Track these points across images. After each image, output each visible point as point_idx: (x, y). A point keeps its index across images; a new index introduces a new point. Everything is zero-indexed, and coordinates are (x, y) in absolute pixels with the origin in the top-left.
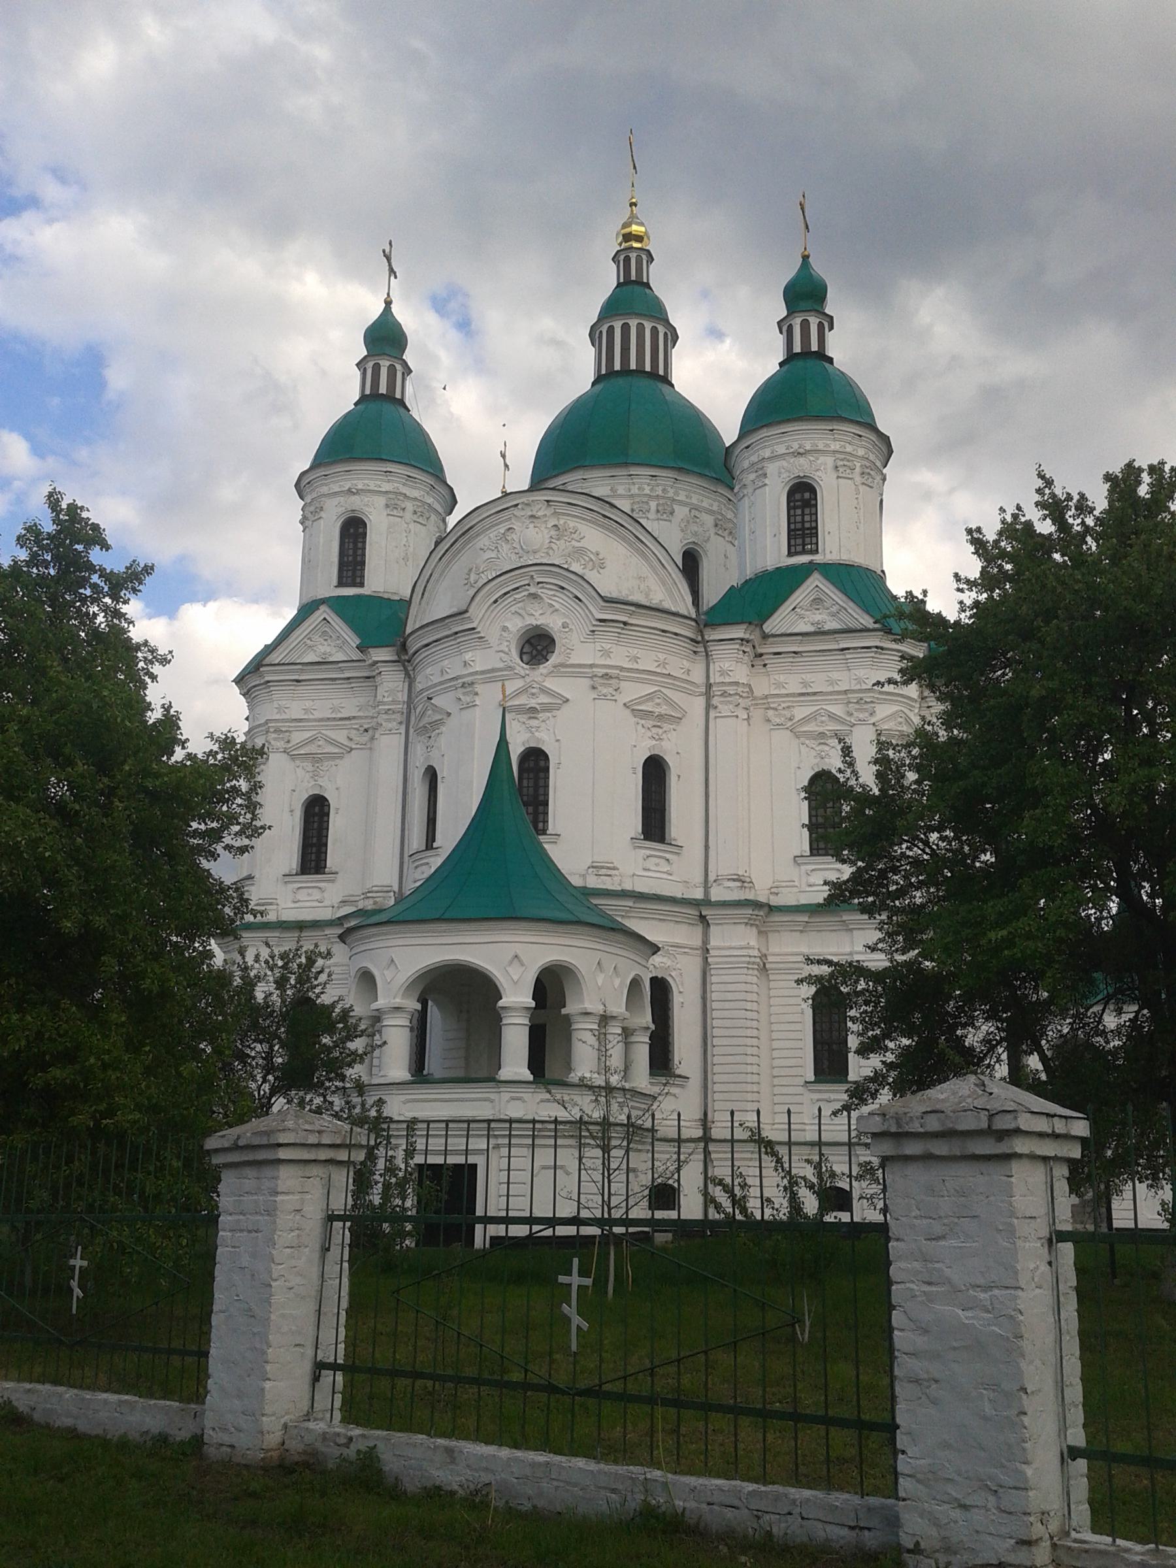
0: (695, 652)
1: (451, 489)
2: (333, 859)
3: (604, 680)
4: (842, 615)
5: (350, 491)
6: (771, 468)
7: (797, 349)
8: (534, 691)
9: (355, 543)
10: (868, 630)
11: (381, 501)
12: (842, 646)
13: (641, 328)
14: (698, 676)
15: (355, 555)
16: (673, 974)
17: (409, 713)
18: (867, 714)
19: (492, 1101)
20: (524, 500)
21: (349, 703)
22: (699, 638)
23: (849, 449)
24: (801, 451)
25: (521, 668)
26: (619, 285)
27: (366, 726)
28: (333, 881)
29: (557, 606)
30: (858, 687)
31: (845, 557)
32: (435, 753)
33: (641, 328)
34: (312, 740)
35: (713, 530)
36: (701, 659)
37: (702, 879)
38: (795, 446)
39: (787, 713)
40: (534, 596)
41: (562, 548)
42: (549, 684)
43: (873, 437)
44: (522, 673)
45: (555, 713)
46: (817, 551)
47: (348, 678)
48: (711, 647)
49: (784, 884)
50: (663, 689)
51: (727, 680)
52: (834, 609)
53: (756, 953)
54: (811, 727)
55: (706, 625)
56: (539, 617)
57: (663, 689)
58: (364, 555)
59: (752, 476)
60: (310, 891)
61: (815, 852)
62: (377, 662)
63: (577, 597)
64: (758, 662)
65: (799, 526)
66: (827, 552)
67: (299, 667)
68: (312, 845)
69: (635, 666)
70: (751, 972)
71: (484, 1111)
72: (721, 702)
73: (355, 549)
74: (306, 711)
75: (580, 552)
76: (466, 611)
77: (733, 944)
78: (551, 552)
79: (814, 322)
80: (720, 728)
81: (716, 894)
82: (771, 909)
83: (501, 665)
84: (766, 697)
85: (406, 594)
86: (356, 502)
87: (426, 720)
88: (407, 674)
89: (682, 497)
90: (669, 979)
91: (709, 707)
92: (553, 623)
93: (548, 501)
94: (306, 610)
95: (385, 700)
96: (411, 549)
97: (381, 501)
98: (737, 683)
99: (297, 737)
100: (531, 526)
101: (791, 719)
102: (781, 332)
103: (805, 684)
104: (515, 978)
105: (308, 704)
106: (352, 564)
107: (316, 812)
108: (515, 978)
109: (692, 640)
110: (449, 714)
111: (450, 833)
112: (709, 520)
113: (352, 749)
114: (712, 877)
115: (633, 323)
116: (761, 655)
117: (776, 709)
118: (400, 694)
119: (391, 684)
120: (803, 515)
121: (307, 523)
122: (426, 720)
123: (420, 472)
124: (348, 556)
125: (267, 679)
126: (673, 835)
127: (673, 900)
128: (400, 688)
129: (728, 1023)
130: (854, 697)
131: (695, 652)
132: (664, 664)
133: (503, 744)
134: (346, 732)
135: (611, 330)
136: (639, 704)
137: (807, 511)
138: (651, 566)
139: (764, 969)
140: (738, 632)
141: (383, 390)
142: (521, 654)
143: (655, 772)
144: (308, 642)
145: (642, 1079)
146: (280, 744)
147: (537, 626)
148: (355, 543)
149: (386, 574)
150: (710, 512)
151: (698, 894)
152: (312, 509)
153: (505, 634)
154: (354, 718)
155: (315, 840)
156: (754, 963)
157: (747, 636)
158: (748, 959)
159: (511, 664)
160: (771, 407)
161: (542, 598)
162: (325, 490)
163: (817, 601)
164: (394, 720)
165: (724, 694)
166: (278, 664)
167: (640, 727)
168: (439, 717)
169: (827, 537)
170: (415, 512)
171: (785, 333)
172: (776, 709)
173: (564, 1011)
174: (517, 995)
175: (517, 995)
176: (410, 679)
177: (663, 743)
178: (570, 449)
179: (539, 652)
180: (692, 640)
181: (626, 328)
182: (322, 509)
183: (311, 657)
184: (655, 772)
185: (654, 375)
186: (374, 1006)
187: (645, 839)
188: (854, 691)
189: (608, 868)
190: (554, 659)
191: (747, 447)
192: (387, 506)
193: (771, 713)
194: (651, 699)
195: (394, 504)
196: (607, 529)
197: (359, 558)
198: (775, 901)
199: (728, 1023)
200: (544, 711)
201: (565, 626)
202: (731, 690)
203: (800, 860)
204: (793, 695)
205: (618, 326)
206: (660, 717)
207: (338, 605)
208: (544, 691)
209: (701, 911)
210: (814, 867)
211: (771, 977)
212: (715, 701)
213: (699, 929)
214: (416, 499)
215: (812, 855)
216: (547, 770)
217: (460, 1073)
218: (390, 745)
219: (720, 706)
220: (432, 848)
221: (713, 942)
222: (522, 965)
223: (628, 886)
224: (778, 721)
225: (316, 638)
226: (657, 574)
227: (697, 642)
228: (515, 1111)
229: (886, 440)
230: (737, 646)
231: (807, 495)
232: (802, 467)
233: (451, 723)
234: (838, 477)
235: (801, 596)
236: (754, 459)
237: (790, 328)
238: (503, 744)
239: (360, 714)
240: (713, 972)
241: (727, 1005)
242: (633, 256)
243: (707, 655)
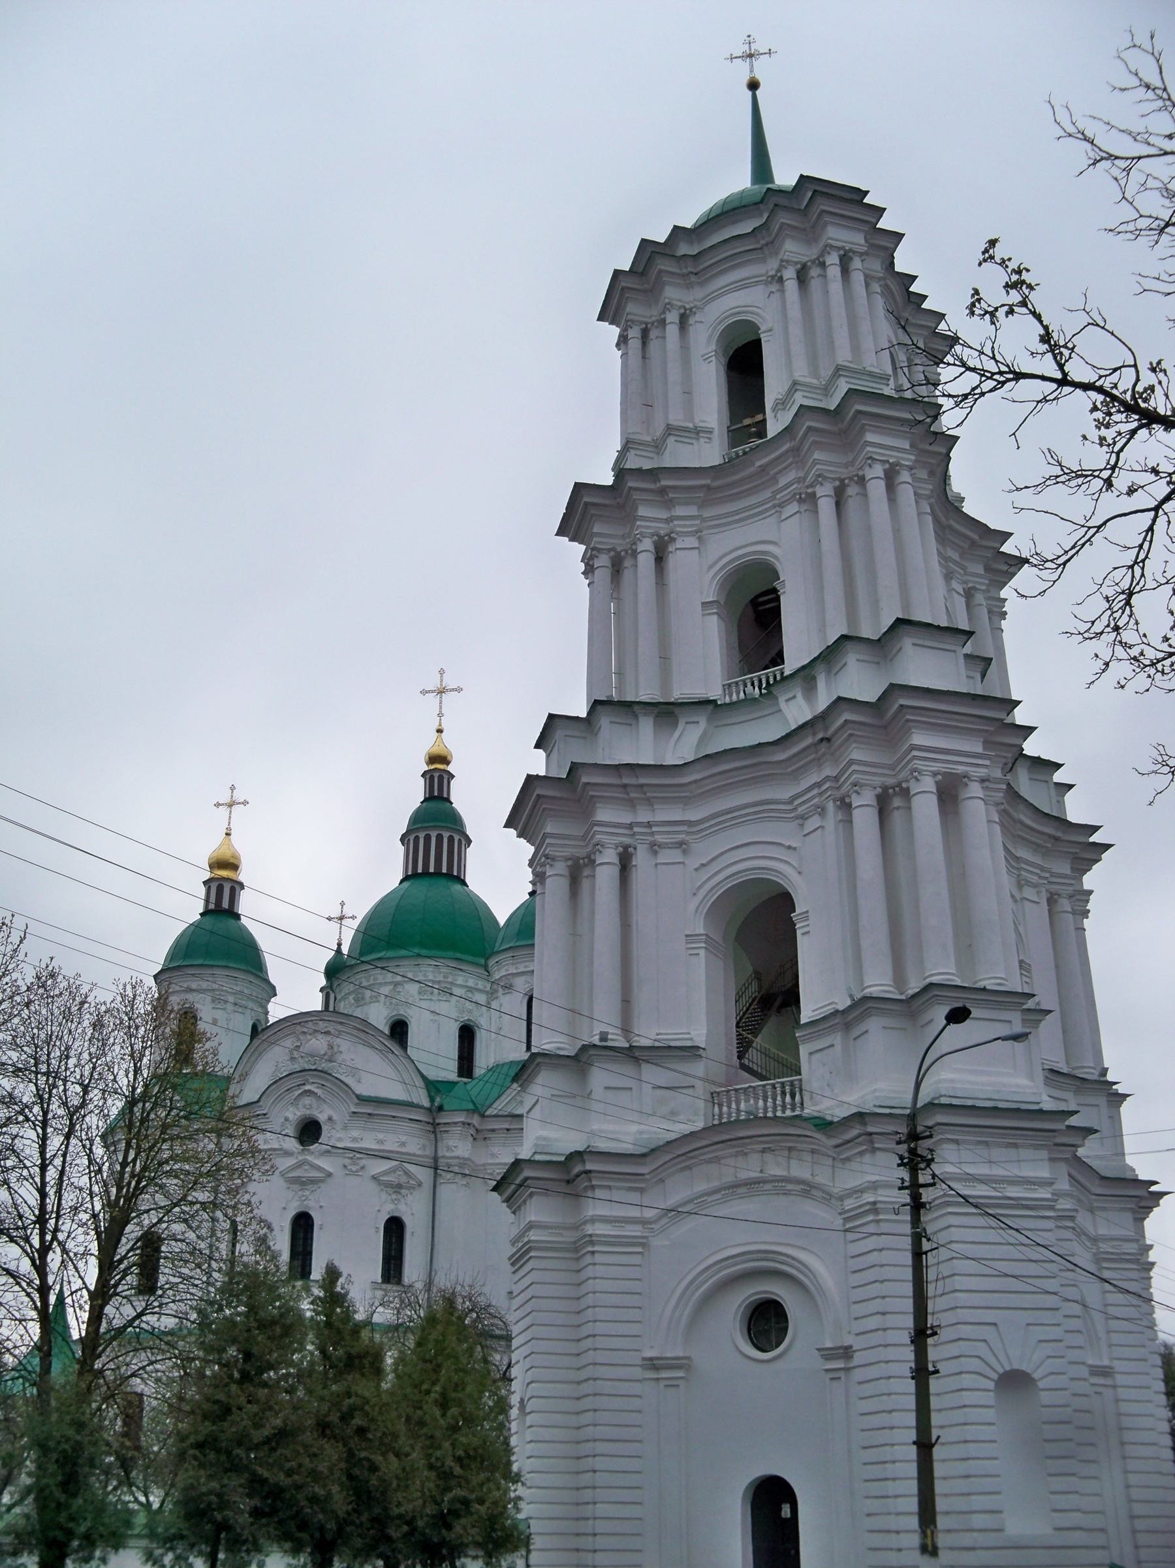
13: (440, 838)
26: (426, 800)
33: (440, 838)
42: (320, 1162)
115: (434, 835)
135: (417, 839)
141: (225, 905)
143: (395, 1229)
181: (428, 838)
184: (395, 1229)
185: (449, 876)
194: (394, 1171)
201: (330, 1119)
205: (422, 835)
206: (400, 1186)
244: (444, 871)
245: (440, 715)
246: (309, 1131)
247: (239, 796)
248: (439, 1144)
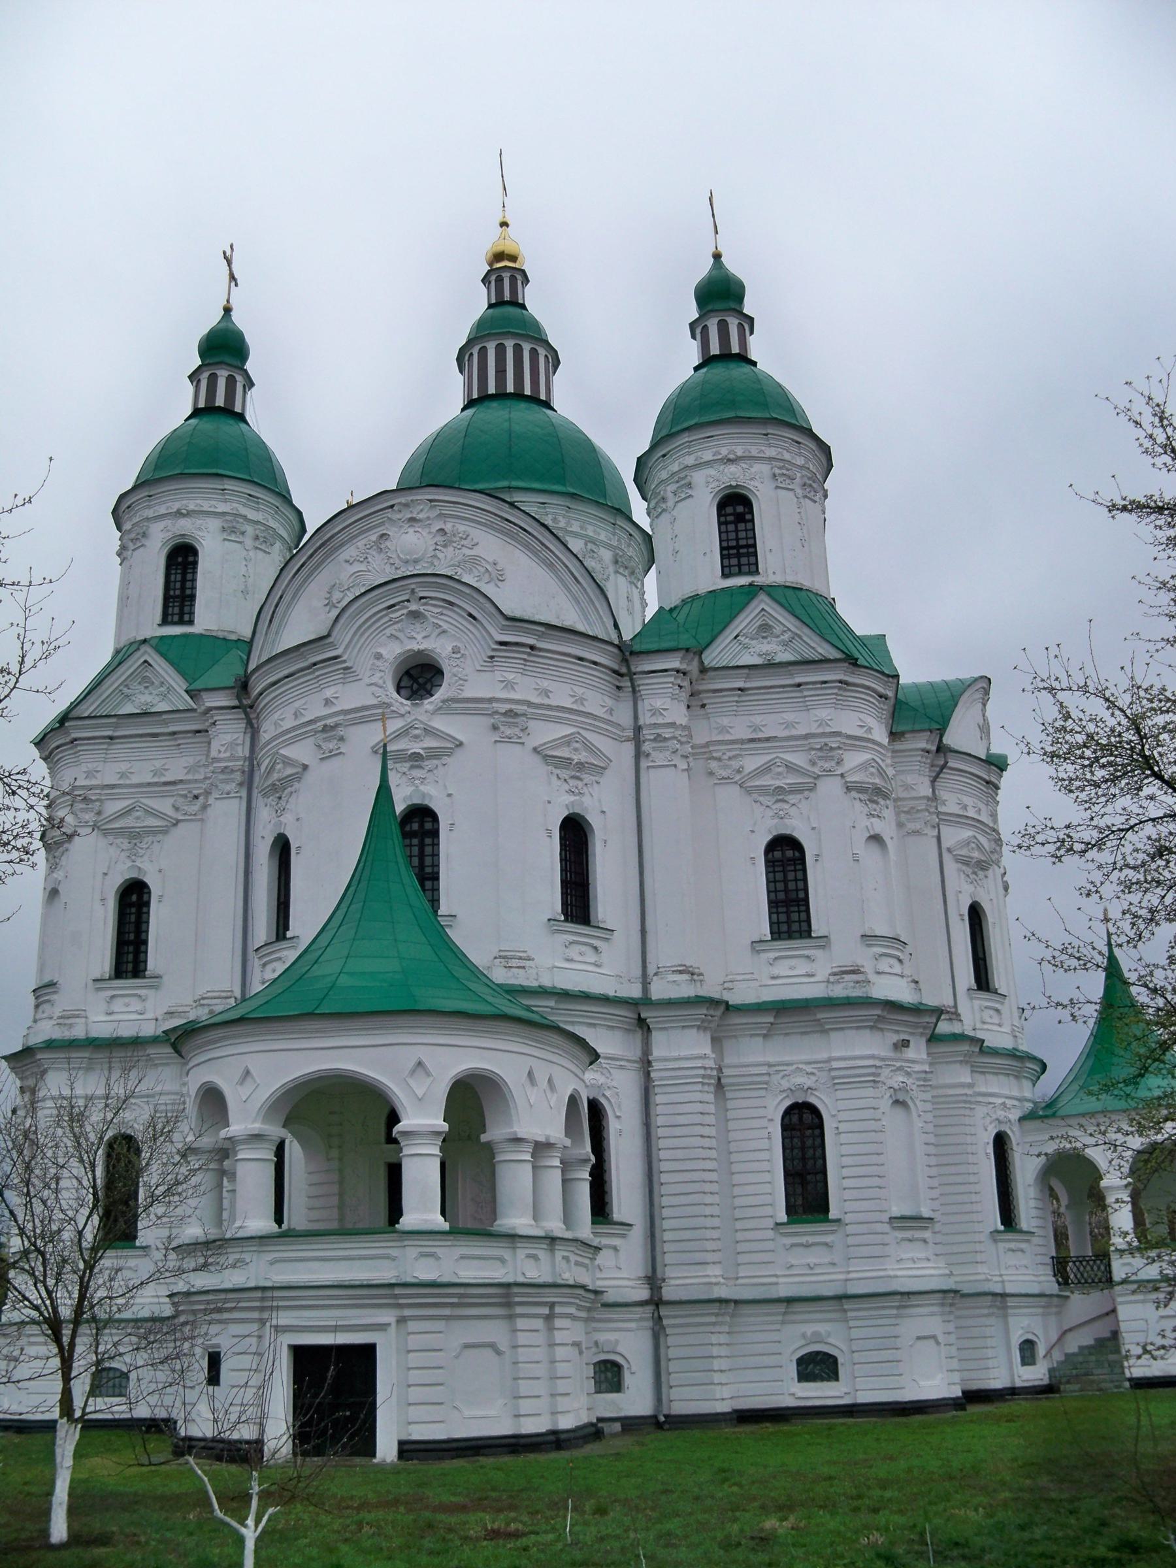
0: (618, 688)
1: (300, 514)
2: (154, 960)
3: (509, 718)
4: (797, 643)
5: (179, 514)
6: (698, 477)
7: (715, 350)
8: (417, 732)
9: (184, 574)
10: (826, 661)
11: (214, 524)
12: (798, 680)
13: (518, 349)
14: (624, 715)
15: (183, 588)
16: (608, 1093)
17: (252, 772)
18: (833, 763)
19: (394, 1259)
20: (403, 500)
21: (177, 764)
22: (624, 670)
23: (787, 456)
24: (731, 456)
25: (401, 703)
26: (490, 306)
27: (196, 792)
28: (155, 988)
29: (445, 626)
30: (820, 730)
31: (790, 579)
32: (288, 818)
33: (518, 349)
34: (128, 812)
35: (611, 569)
36: (627, 694)
37: (639, 972)
38: (724, 451)
39: (735, 764)
40: (415, 615)
41: (449, 557)
42: (439, 723)
43: (812, 445)
44: (402, 711)
45: (445, 760)
46: (757, 572)
47: (174, 733)
48: (640, 681)
49: (739, 977)
50: (582, 732)
51: (660, 721)
52: (786, 636)
53: (711, 1064)
54: (767, 781)
55: (632, 653)
56: (421, 640)
57: (582, 732)
58: (194, 588)
59: (672, 488)
60: (127, 1000)
61: (776, 936)
62: (210, 709)
63: (470, 615)
64: (696, 702)
65: (734, 543)
66: (770, 572)
67: (114, 720)
68: (129, 943)
69: (546, 701)
70: (706, 1088)
71: (384, 1273)
72: (654, 749)
73: (184, 581)
74: (123, 775)
75: (475, 561)
76: (329, 635)
77: (682, 1054)
78: (436, 562)
79: (733, 323)
80: (653, 780)
81: (658, 991)
82: (728, 1007)
83: (374, 702)
84: (707, 745)
85: (247, 633)
86: (185, 526)
87: (275, 776)
88: (250, 723)
89: (575, 527)
90: (603, 1100)
91: (638, 755)
92: (440, 648)
93: (431, 501)
94: (121, 656)
95: (222, 755)
96: (250, 580)
97: (214, 524)
98: (672, 725)
99: (112, 807)
100: (411, 530)
101: (739, 772)
102: (693, 337)
103: (756, 729)
104: (420, 1093)
105: (123, 767)
106: (179, 599)
107: (133, 900)
108: (420, 1093)
109: (615, 672)
110: (305, 767)
111: (310, 913)
112: (607, 555)
113: (178, 821)
114: (651, 970)
115: (509, 344)
116: (700, 692)
117: (719, 759)
118: (240, 748)
119: (228, 736)
120: (737, 531)
121: (125, 554)
122: (276, 776)
123: (264, 491)
124: (175, 589)
125: (74, 735)
126: (600, 916)
127: (605, 1000)
128: (240, 741)
129: (679, 1154)
130: (817, 743)
131: (618, 688)
132: (582, 700)
133: (384, 792)
134: (172, 800)
135: (483, 352)
136: (552, 748)
137: (741, 526)
138: (561, 580)
139: (720, 1085)
140: (673, 662)
142: (399, 689)
143: (575, 835)
144: (125, 690)
145: (584, 1228)
146: (89, 817)
147: (420, 652)
148: (184, 574)
149: (220, 609)
150: (608, 546)
151: (635, 992)
152: (133, 536)
153: (378, 663)
154: (181, 781)
155: (132, 937)
156: (710, 1077)
157: (683, 667)
158: (702, 1072)
159: (387, 700)
160: (682, 419)
161: (425, 617)
162: (150, 513)
163: (765, 630)
164: (232, 780)
165: (658, 738)
166: (89, 717)
167: (554, 778)
168: (289, 771)
169: (769, 556)
170: (257, 538)
171: (698, 336)
172: (719, 759)
173: (484, 1138)
174: (423, 1117)
175: (423, 1117)
176: (253, 729)
177: (584, 799)
178: (443, 470)
179: (422, 687)
180: (615, 672)
182: (144, 535)
183: (128, 709)
184: (575, 835)
185: (534, 399)
186: (223, 1133)
187: (566, 920)
188: (813, 735)
189: (520, 958)
190: (440, 694)
191: (664, 456)
192: (224, 529)
193: (714, 765)
195: (232, 528)
196: (506, 534)
197: (188, 592)
198: (734, 999)
199: (679, 1154)
200: (430, 757)
201: (456, 650)
202: (667, 732)
203: (758, 947)
204: (742, 742)
206: (581, 766)
207: (161, 645)
208: (429, 731)
209: (639, 1015)
210: (777, 954)
211: (729, 1095)
212: (646, 747)
213: (639, 1036)
214: (257, 522)
215: (773, 939)
216: (435, 833)
217: (334, 1225)
218: (226, 813)
219: (653, 754)
220: (284, 938)
221: (657, 1052)
222: (428, 1074)
223: (546, 982)
224: (724, 774)
225: (135, 685)
226: (570, 591)
227: (621, 675)
228: (425, 1272)
229: (826, 450)
230: (672, 679)
231: (740, 509)
232: (732, 475)
233: (310, 778)
234: (777, 487)
235: (745, 622)
236: (675, 467)
237: (705, 329)
238: (384, 792)
239: (190, 777)
240: (657, 1090)
241: (677, 1131)
242: (506, 276)
243: (634, 691)
244: (527, 392)
246: (419, 677)
248: (640, 703)
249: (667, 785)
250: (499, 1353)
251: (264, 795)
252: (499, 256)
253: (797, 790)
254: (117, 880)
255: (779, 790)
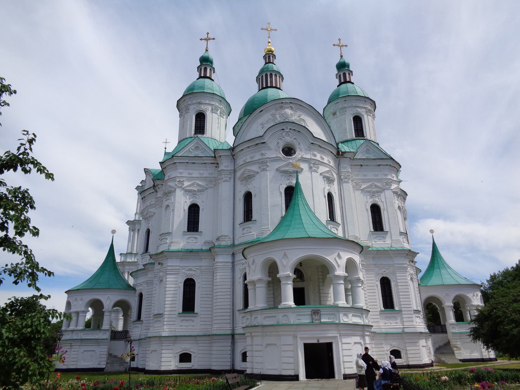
2: (201, 227)
11: (210, 108)
21: (207, 172)
86: (203, 107)
107: (194, 211)
125: (175, 161)
132: (330, 162)
135: (266, 75)
217: (272, 306)
245: (269, 37)
247: (210, 36)
249: (348, 187)
250: (362, 345)
251: (241, 181)
252: (268, 51)
253: (378, 192)
254: (189, 204)
255: (374, 192)
